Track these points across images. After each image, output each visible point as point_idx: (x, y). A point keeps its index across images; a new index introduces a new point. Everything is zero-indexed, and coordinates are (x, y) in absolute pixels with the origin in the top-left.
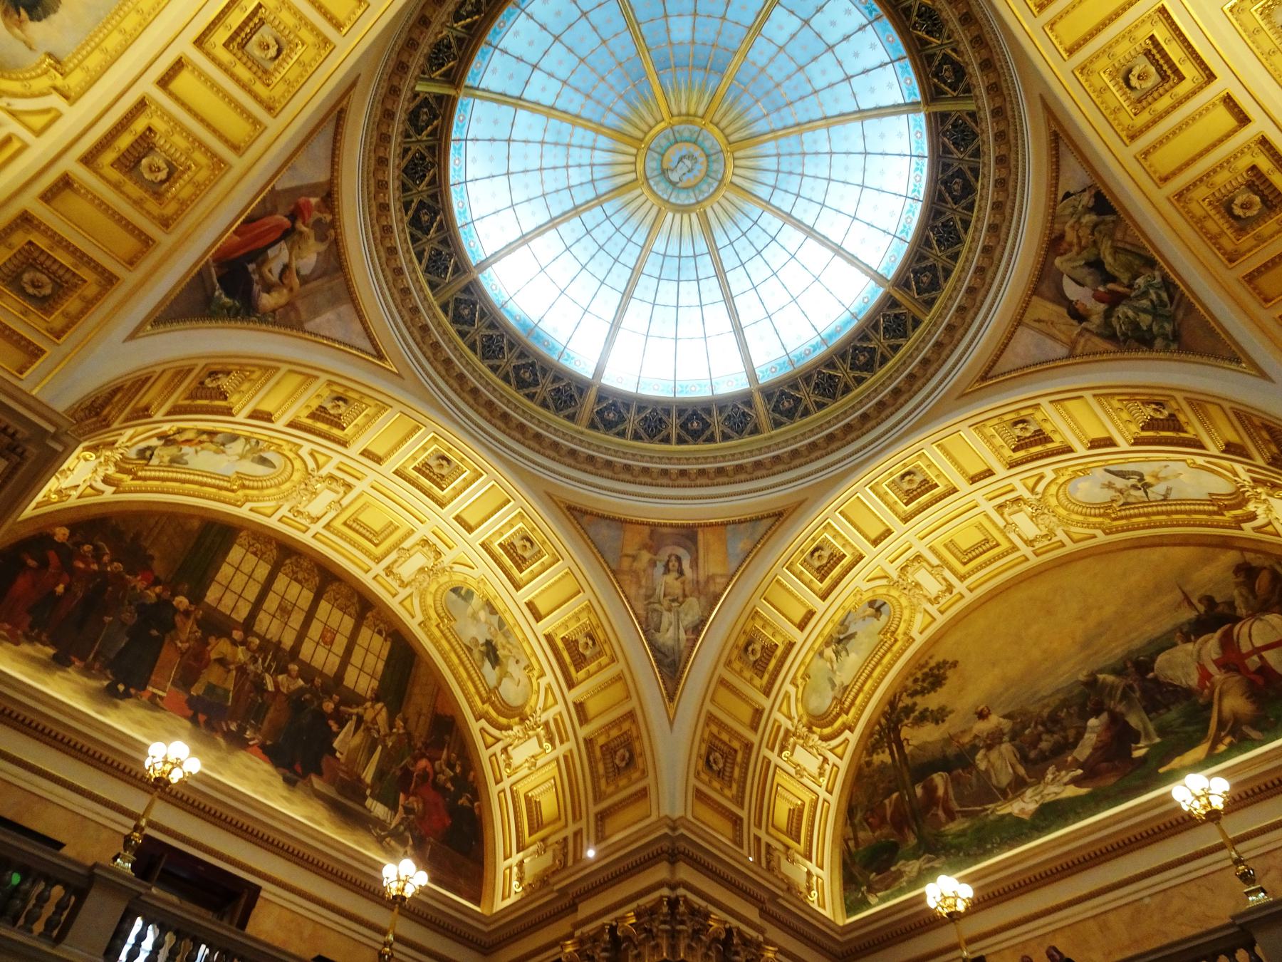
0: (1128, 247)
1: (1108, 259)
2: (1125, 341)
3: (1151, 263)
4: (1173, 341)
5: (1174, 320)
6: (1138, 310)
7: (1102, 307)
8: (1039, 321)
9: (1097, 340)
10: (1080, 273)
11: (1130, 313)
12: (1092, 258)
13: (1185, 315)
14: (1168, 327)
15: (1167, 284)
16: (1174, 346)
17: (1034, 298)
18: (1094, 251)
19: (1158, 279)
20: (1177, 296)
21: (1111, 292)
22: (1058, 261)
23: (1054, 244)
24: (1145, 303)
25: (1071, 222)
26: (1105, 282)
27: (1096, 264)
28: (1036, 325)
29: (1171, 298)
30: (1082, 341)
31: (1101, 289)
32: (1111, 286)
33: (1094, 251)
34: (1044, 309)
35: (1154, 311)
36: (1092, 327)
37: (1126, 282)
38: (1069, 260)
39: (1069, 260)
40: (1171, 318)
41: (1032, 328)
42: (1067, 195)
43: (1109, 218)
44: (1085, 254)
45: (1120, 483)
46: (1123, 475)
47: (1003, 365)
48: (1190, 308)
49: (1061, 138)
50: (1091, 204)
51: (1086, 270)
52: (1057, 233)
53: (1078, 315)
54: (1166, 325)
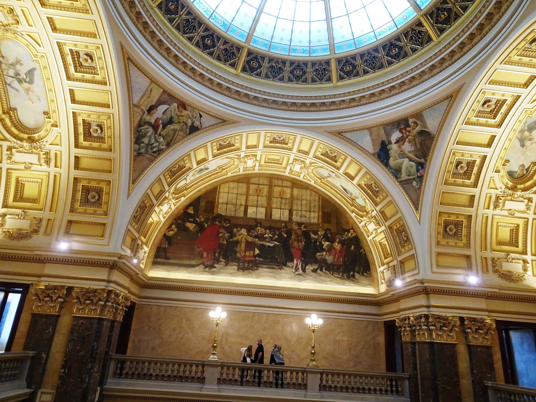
0: (176, 136)
1: (172, 127)
2: (137, 131)
3: (168, 145)
4: (137, 153)
5: (146, 153)
6: (150, 137)
7: (153, 121)
8: (151, 90)
9: (139, 117)
10: (168, 113)
11: (149, 134)
12: (173, 120)
13: (148, 158)
14: (143, 150)
15: (160, 152)
16: (135, 153)
17: (162, 90)
18: (176, 122)
19: (162, 147)
20: (155, 155)
21: (158, 126)
22: (175, 105)
23: (183, 105)
24: (153, 141)
25: (190, 115)
26: (163, 124)
27: (171, 121)
28: (149, 89)
29: (154, 152)
30: (139, 111)
31: (160, 122)
32: (161, 126)
33: (176, 122)
34: (156, 95)
35: (149, 144)
36: (145, 116)
37: (162, 133)
38: (175, 110)
39: (175, 110)
40: (147, 152)
41: (148, 87)
42: (201, 116)
43: (188, 131)
44: (176, 117)
45: (23, 71)
46: (30, 73)
47: (132, 67)
48: (151, 161)
49: (223, 122)
50: (195, 125)
51: (169, 116)
52: (187, 108)
53: (151, 109)
54: (144, 150)
